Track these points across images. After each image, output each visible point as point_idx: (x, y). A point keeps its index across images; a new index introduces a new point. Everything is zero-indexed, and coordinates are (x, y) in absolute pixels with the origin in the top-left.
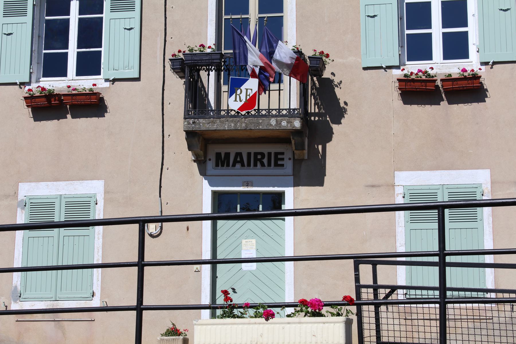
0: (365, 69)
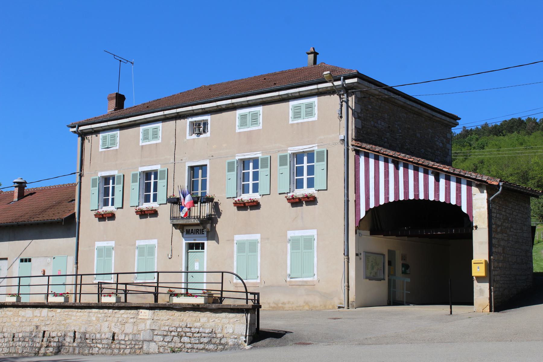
0: (227, 198)
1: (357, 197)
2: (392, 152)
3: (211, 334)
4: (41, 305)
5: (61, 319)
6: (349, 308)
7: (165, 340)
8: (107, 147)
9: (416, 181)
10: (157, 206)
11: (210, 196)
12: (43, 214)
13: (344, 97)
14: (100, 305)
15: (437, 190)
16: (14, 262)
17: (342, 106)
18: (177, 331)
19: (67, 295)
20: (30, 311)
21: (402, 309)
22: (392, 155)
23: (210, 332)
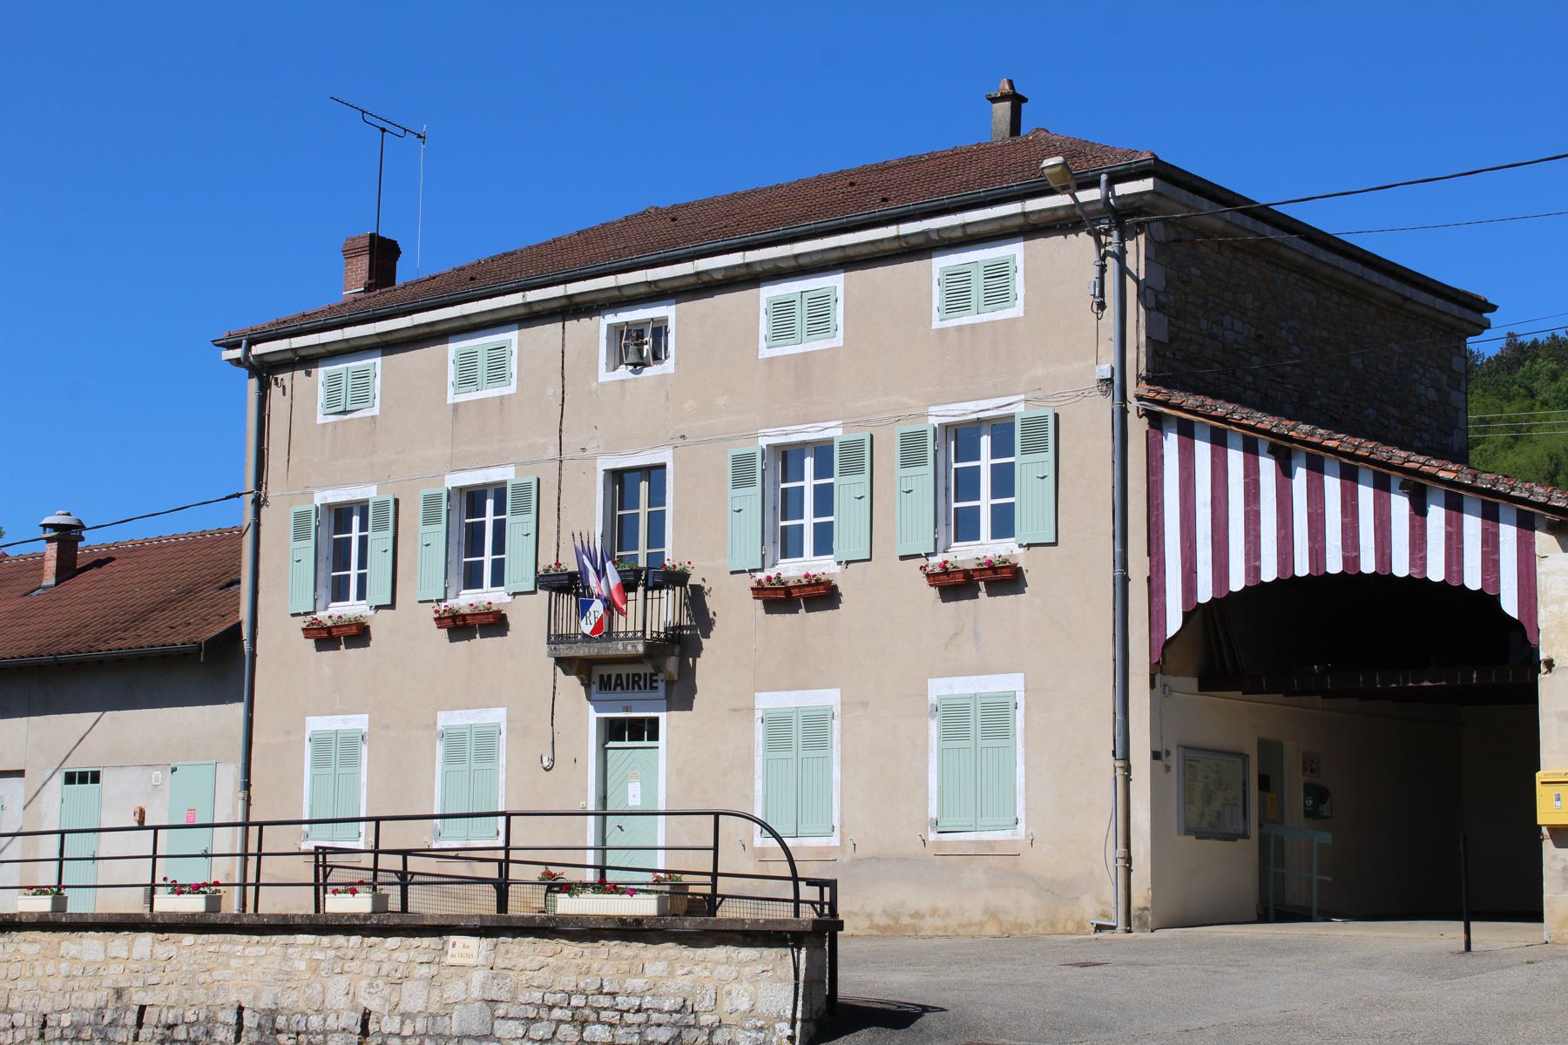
0: (732, 573)
1: (1155, 568)
2: (1271, 418)
3: (679, 1016)
4: (131, 920)
5: (196, 967)
6: (1130, 931)
7: (532, 1034)
8: (341, 409)
9: (1349, 512)
10: (504, 601)
11: (674, 566)
12: (138, 629)
13: (1109, 239)
14: (321, 921)
15: (1418, 542)
16: (44, 785)
17: (1103, 269)
18: (569, 1004)
19: (213, 888)
20: (95, 941)
21: (1306, 932)
22: (1269, 427)
23: (678, 1007)
